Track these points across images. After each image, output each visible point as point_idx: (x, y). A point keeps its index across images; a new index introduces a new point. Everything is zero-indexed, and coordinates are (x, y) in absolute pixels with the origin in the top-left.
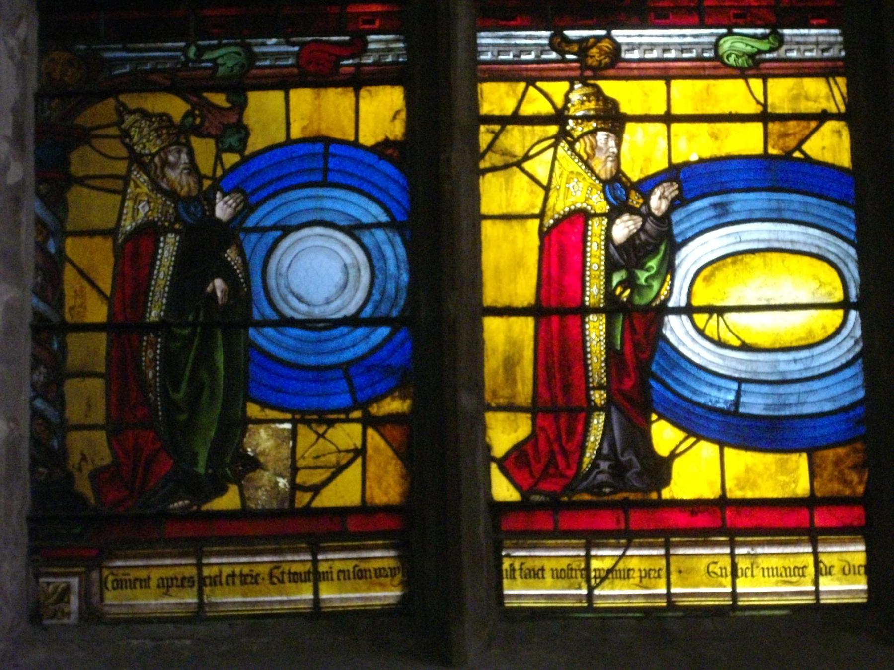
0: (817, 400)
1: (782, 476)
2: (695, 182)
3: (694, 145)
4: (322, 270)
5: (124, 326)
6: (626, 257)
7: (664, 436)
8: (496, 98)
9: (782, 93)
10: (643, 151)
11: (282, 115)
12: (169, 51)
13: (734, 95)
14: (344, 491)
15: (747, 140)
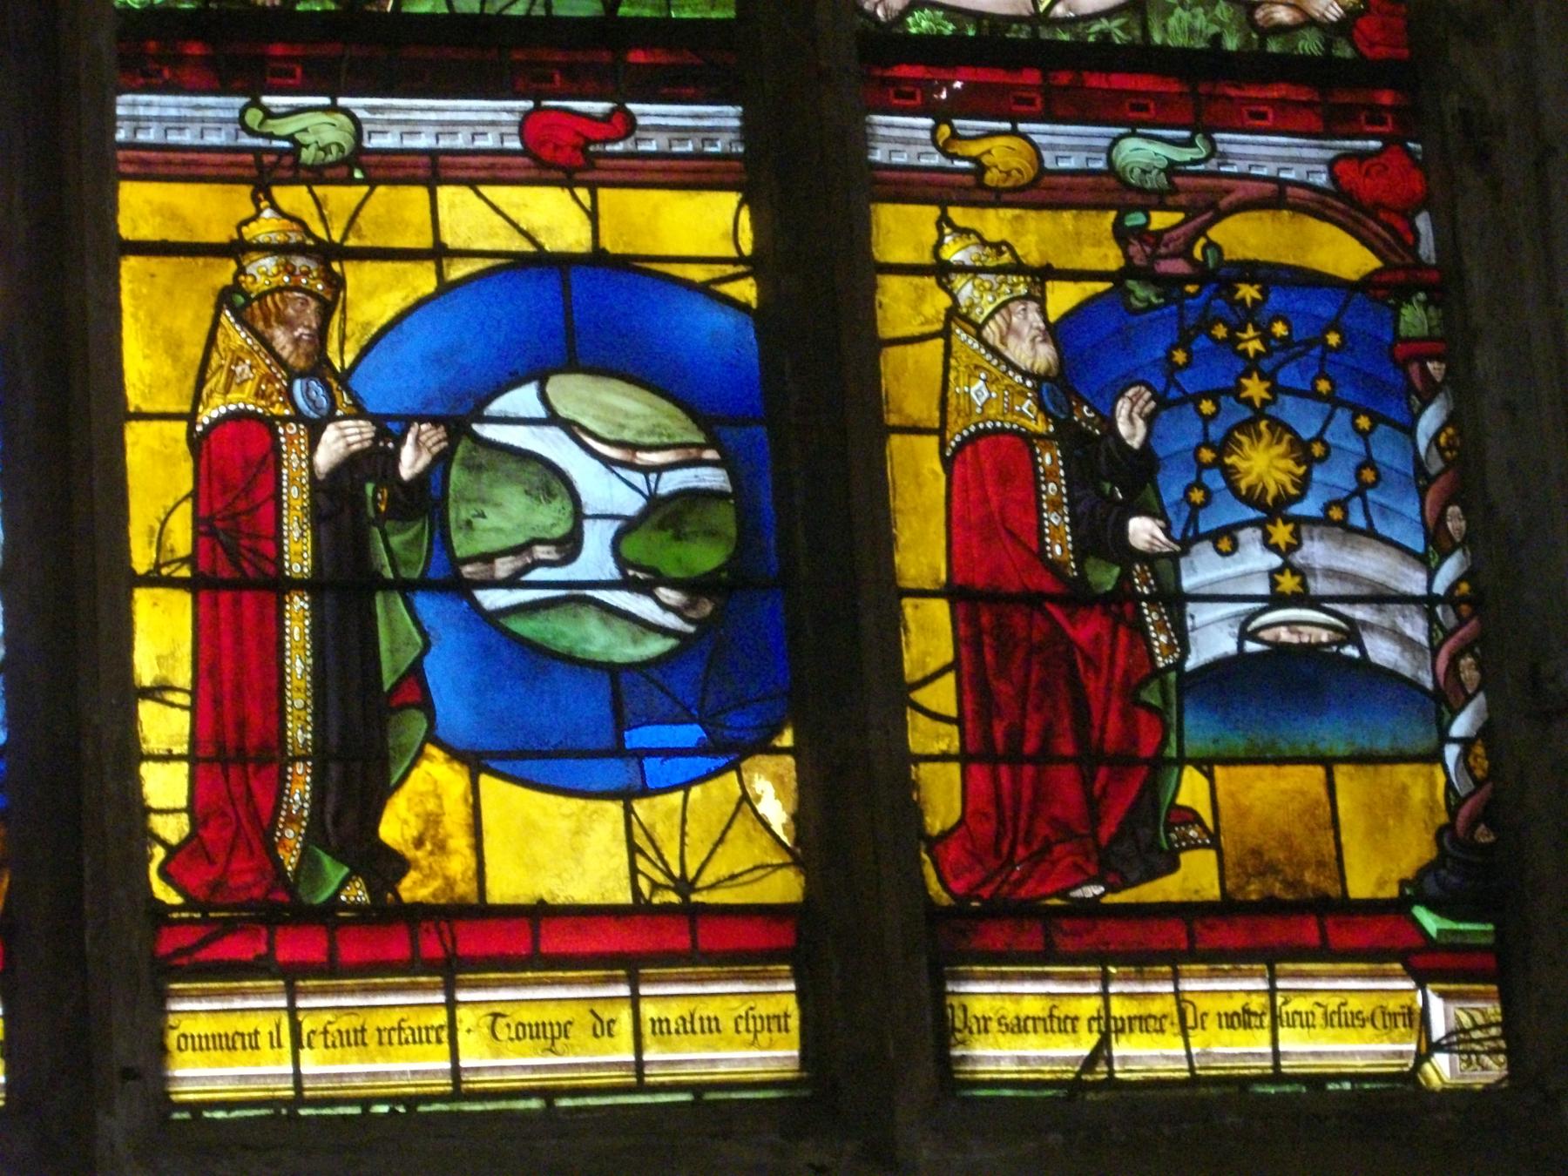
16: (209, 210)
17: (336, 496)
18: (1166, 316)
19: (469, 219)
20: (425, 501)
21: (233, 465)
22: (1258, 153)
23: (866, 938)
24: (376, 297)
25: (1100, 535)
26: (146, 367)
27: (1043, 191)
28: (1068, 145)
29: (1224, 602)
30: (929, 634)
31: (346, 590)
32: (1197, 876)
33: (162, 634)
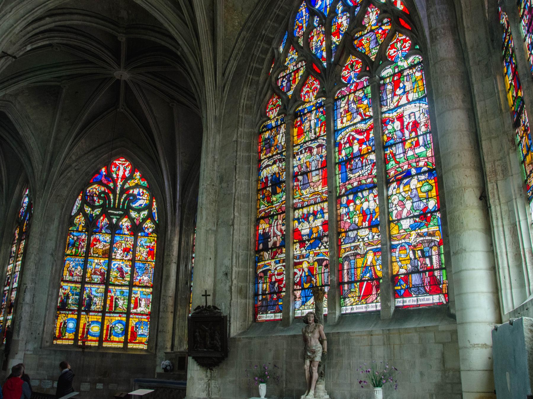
0: (97, 335)
1: (95, 338)
2: (93, 322)
3: (93, 320)
4: (71, 325)
5: (60, 327)
6: (88, 326)
7: (88, 336)
8: (82, 316)
9: (98, 317)
10: (90, 320)
11: (70, 316)
12: (64, 312)
13: (95, 317)
14: (71, 338)
15: (95, 320)
16: (108, 318)
17: (111, 327)
18: (140, 322)
19: (117, 318)
20: (114, 328)
21: (108, 326)
22: (144, 317)
23: (126, 342)
24: (113, 321)
25: (136, 330)
26: (105, 323)
27: (136, 318)
28: (137, 316)
29: (140, 332)
30: (129, 333)
31: (111, 330)
32: (137, 341)
33: (105, 332)
